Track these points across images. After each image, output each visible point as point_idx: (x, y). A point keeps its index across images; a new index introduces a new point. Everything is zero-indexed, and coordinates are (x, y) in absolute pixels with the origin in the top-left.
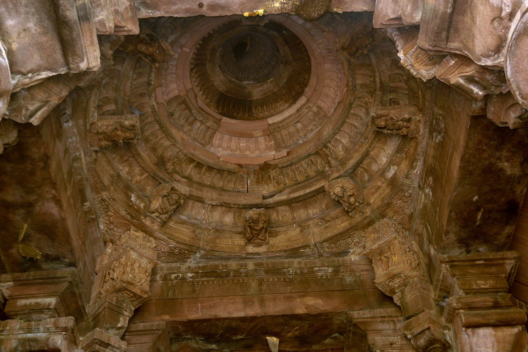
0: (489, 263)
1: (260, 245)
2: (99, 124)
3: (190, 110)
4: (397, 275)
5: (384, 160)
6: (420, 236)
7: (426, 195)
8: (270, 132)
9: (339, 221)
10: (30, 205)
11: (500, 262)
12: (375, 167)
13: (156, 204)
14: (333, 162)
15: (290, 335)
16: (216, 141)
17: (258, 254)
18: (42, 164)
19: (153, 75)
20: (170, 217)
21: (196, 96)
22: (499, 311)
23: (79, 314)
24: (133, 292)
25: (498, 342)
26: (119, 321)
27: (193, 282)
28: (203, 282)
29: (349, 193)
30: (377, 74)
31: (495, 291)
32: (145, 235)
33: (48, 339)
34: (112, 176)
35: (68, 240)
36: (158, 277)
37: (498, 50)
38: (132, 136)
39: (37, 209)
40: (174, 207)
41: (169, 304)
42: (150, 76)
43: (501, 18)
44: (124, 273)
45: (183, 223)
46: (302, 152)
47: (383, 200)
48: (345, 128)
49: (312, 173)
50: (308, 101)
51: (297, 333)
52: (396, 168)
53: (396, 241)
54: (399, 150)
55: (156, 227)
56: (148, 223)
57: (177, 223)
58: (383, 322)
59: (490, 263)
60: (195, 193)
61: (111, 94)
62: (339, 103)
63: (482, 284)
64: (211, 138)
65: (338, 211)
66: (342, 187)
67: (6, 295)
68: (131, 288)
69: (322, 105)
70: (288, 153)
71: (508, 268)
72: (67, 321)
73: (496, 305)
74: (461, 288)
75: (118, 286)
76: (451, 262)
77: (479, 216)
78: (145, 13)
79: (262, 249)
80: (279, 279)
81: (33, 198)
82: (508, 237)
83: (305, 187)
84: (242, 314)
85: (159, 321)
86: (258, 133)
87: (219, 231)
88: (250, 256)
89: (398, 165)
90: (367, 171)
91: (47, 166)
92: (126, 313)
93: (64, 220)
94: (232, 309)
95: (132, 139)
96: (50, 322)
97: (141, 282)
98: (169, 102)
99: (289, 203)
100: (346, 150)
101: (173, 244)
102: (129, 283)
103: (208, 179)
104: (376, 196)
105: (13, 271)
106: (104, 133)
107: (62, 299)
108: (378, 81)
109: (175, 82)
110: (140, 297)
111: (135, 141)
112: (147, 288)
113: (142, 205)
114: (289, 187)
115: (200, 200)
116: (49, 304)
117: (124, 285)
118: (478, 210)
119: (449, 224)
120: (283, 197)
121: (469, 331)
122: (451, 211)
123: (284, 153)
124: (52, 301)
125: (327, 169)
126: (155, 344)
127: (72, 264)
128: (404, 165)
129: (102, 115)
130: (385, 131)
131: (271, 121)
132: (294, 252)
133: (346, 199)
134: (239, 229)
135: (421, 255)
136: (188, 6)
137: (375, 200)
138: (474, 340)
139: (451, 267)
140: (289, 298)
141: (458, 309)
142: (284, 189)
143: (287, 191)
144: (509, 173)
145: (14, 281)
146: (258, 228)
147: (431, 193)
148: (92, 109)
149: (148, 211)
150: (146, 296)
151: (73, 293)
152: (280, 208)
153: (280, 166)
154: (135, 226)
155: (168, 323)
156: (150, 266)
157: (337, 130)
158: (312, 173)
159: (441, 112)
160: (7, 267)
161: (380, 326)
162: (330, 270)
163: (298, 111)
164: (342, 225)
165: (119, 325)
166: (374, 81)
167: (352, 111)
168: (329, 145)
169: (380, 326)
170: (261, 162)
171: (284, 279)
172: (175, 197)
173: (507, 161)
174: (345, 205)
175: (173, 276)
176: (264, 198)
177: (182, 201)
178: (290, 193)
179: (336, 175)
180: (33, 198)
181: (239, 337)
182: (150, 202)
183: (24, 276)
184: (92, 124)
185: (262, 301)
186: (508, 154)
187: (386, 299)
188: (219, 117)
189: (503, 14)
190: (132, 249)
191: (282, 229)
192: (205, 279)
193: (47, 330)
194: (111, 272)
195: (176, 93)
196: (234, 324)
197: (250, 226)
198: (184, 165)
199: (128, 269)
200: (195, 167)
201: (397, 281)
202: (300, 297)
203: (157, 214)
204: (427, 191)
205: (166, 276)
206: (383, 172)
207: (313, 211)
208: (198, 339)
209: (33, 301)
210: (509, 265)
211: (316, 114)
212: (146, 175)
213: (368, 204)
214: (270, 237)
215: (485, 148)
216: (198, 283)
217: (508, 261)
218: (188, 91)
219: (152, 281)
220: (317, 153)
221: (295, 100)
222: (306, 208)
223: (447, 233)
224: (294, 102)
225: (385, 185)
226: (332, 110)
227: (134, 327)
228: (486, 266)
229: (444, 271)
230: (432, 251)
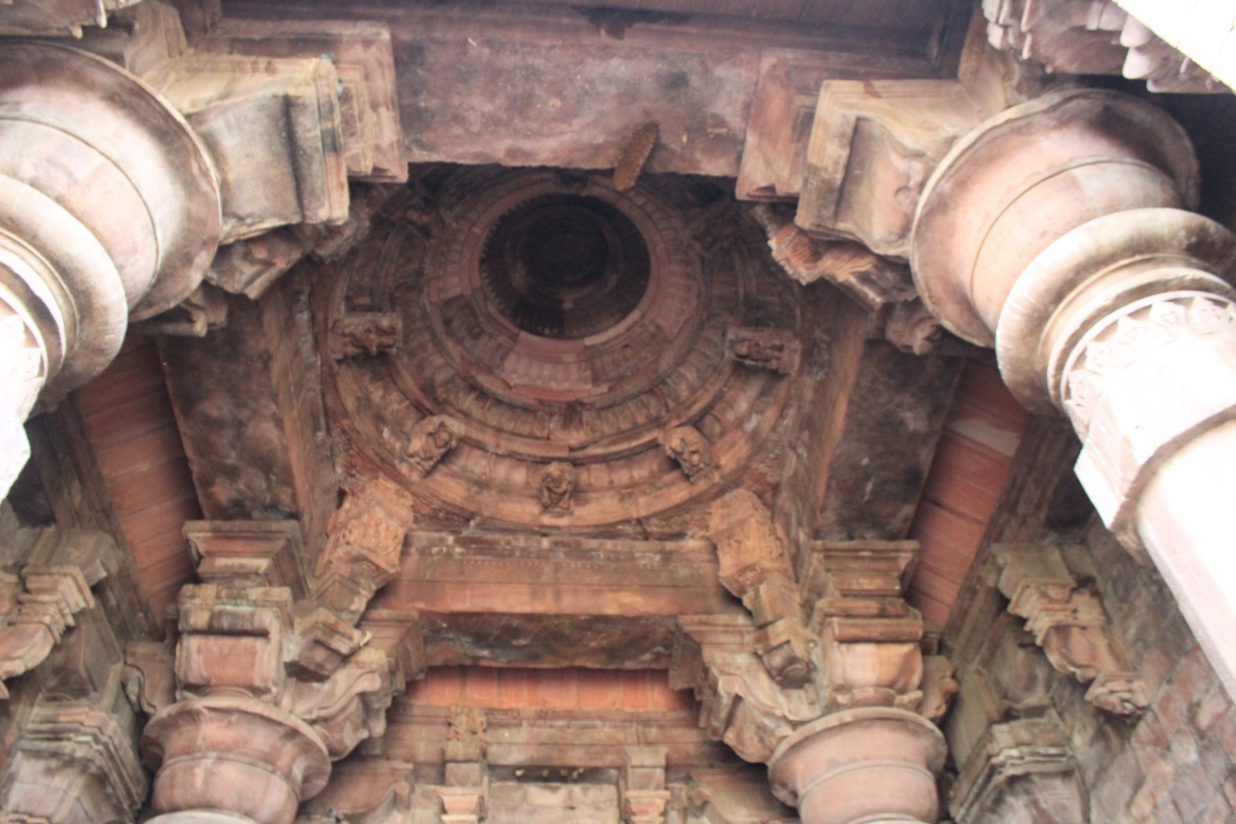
0: (878, 556)
1: (560, 515)
2: (347, 322)
3: (476, 317)
4: (751, 567)
5: (743, 405)
6: (787, 516)
7: (799, 456)
8: (589, 357)
9: (674, 489)
10: (241, 424)
11: (893, 555)
12: (730, 416)
13: (417, 444)
14: (672, 405)
15: (593, 644)
16: (510, 363)
17: (557, 528)
18: (260, 365)
19: (427, 260)
20: (434, 467)
21: (485, 299)
22: (886, 621)
23: (299, 590)
24: (373, 563)
25: (881, 663)
26: (352, 602)
27: (461, 561)
28: (476, 561)
29: (693, 449)
30: (741, 282)
31: (880, 595)
32: (398, 487)
33: (253, 614)
34: (358, 399)
35: (288, 480)
36: (413, 550)
38: (390, 341)
39: (250, 430)
40: (443, 451)
41: (427, 587)
42: (422, 261)
44: (364, 535)
45: (454, 475)
46: (629, 388)
47: (738, 461)
48: (693, 358)
49: (641, 420)
50: (642, 317)
51: (604, 642)
52: (759, 417)
53: (752, 520)
54: (764, 393)
55: (415, 477)
56: (404, 469)
57: (446, 475)
58: (726, 632)
59: (878, 555)
60: (475, 434)
61: (367, 281)
62: (686, 322)
63: (867, 584)
64: (503, 359)
65: (674, 475)
66: (683, 440)
67: (202, 550)
68: (372, 557)
69: (662, 323)
70: (610, 389)
71: (903, 564)
72: (283, 593)
73: (882, 614)
74: (836, 588)
75: (355, 553)
76: (828, 554)
77: (869, 487)
79: (563, 522)
80: (584, 566)
81: (244, 414)
82: (905, 521)
83: (629, 438)
84: (527, 609)
85: (410, 606)
86: (569, 358)
87: (505, 490)
88: (544, 532)
89: (761, 412)
90: (718, 420)
91: (266, 368)
92: (363, 592)
93: (286, 449)
94: (511, 599)
95: (390, 346)
96: (255, 593)
97: (387, 557)
98: (447, 303)
99: (605, 459)
100: (693, 390)
101: (436, 504)
102: (370, 550)
103: (493, 417)
104: (729, 455)
105: (214, 518)
106: (352, 335)
107: (277, 562)
108: (741, 290)
109: (458, 276)
110: (385, 571)
111: (394, 350)
112: (396, 561)
113: (398, 445)
114: (607, 436)
115: (479, 446)
116: (258, 568)
117: (364, 552)
118: (867, 479)
119: (826, 497)
120: (599, 451)
121: (844, 647)
122: (830, 478)
123: (605, 388)
124: (263, 564)
125: (663, 413)
126: (402, 640)
127: (294, 516)
128: (771, 414)
129: (353, 309)
130: (748, 362)
131: (589, 341)
132: (608, 531)
133: (686, 456)
134: (533, 492)
135: (785, 541)
137: (728, 461)
138: (849, 659)
139: (826, 558)
140: (598, 592)
141: (831, 615)
142: (601, 439)
143: (604, 442)
145: (214, 530)
146: (560, 491)
147: (805, 455)
148: (339, 300)
149: (406, 456)
150: (392, 571)
151: (292, 556)
152: (593, 466)
153: (598, 405)
154: (385, 474)
155: (422, 613)
156: (401, 532)
157: (681, 361)
158: (641, 420)
159: (825, 337)
160: (206, 513)
161: (722, 638)
163: (628, 330)
164: (679, 493)
165: (353, 607)
166: (736, 293)
167: (704, 334)
168: (668, 381)
169: (722, 638)
170: (571, 398)
171: (592, 566)
172: (445, 436)
173: (910, 410)
174: (685, 465)
175: (435, 550)
176: (571, 449)
177: (454, 443)
178: (609, 445)
179: (676, 423)
180: (244, 414)
181: (522, 642)
182: (409, 441)
183: (226, 525)
184: (336, 322)
185: (558, 595)
187: (733, 601)
188: (515, 330)
190: (378, 503)
191: (594, 495)
192: (479, 557)
193: (255, 603)
194: (347, 533)
195: (456, 292)
196: (515, 623)
197: (549, 489)
198: (461, 395)
199: (371, 531)
200: (477, 399)
201: (750, 575)
202: (613, 591)
203: (418, 459)
204: (800, 450)
205: (424, 548)
206: (740, 423)
207: (640, 473)
208: (463, 640)
210: (904, 560)
211: (653, 335)
212: (407, 403)
213: (718, 467)
214: (576, 505)
215: (881, 388)
216: (468, 561)
217: (902, 555)
218: (474, 290)
219: (404, 554)
220: (650, 392)
221: (625, 313)
222: (630, 468)
223: (823, 509)
224: (623, 318)
225: (742, 441)
226: (676, 331)
227: (375, 614)
228: (872, 559)
229: (815, 563)
230: (802, 537)
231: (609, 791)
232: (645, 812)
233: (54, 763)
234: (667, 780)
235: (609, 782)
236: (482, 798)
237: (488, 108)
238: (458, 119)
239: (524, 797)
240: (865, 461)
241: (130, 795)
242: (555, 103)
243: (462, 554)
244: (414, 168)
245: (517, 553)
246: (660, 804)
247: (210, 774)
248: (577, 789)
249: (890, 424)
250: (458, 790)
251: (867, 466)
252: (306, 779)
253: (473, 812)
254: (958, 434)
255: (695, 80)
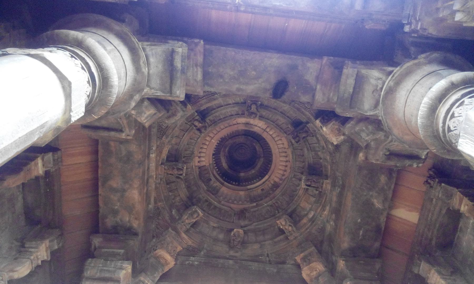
1: (237, 252)
10: (124, 191)
37: (376, 105)
43: (376, 90)
77: (361, 232)
78: (207, 88)
87: (216, 240)
118: (360, 229)
132: (255, 259)
136: (227, 88)
144: (377, 206)
152: (249, 234)
162: (275, 271)
180: (127, 186)
186: (376, 194)
189: (378, 88)
209: (111, 250)
237: (232, 73)
238: (221, 76)
240: (359, 220)
242: (254, 73)
243: (197, 265)
244: (204, 92)
245: (220, 266)
249: (368, 204)
251: (360, 223)
254: (394, 216)
255: (300, 68)
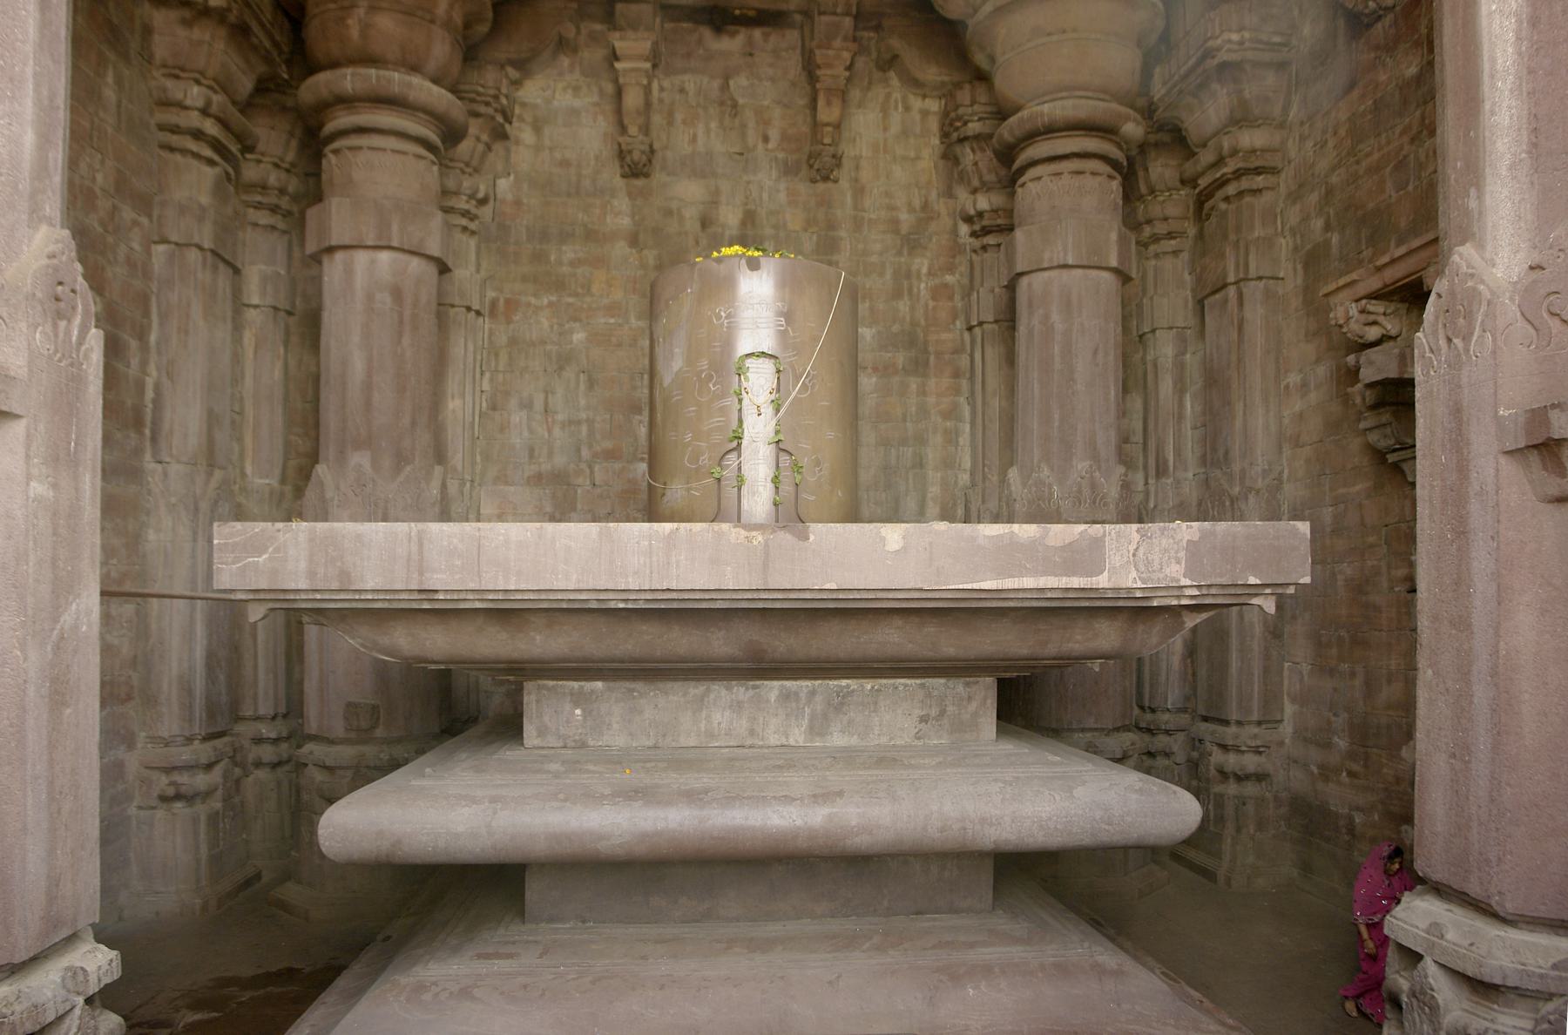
231: (792, 36)
232: (829, 66)
233: (187, 14)
234: (856, 28)
235: (792, 26)
236: (655, 44)
239: (700, 41)
241: (276, 44)
246: (847, 55)
247: (366, 27)
248: (757, 33)
250: (630, 34)
252: (467, 25)
253: (647, 60)
